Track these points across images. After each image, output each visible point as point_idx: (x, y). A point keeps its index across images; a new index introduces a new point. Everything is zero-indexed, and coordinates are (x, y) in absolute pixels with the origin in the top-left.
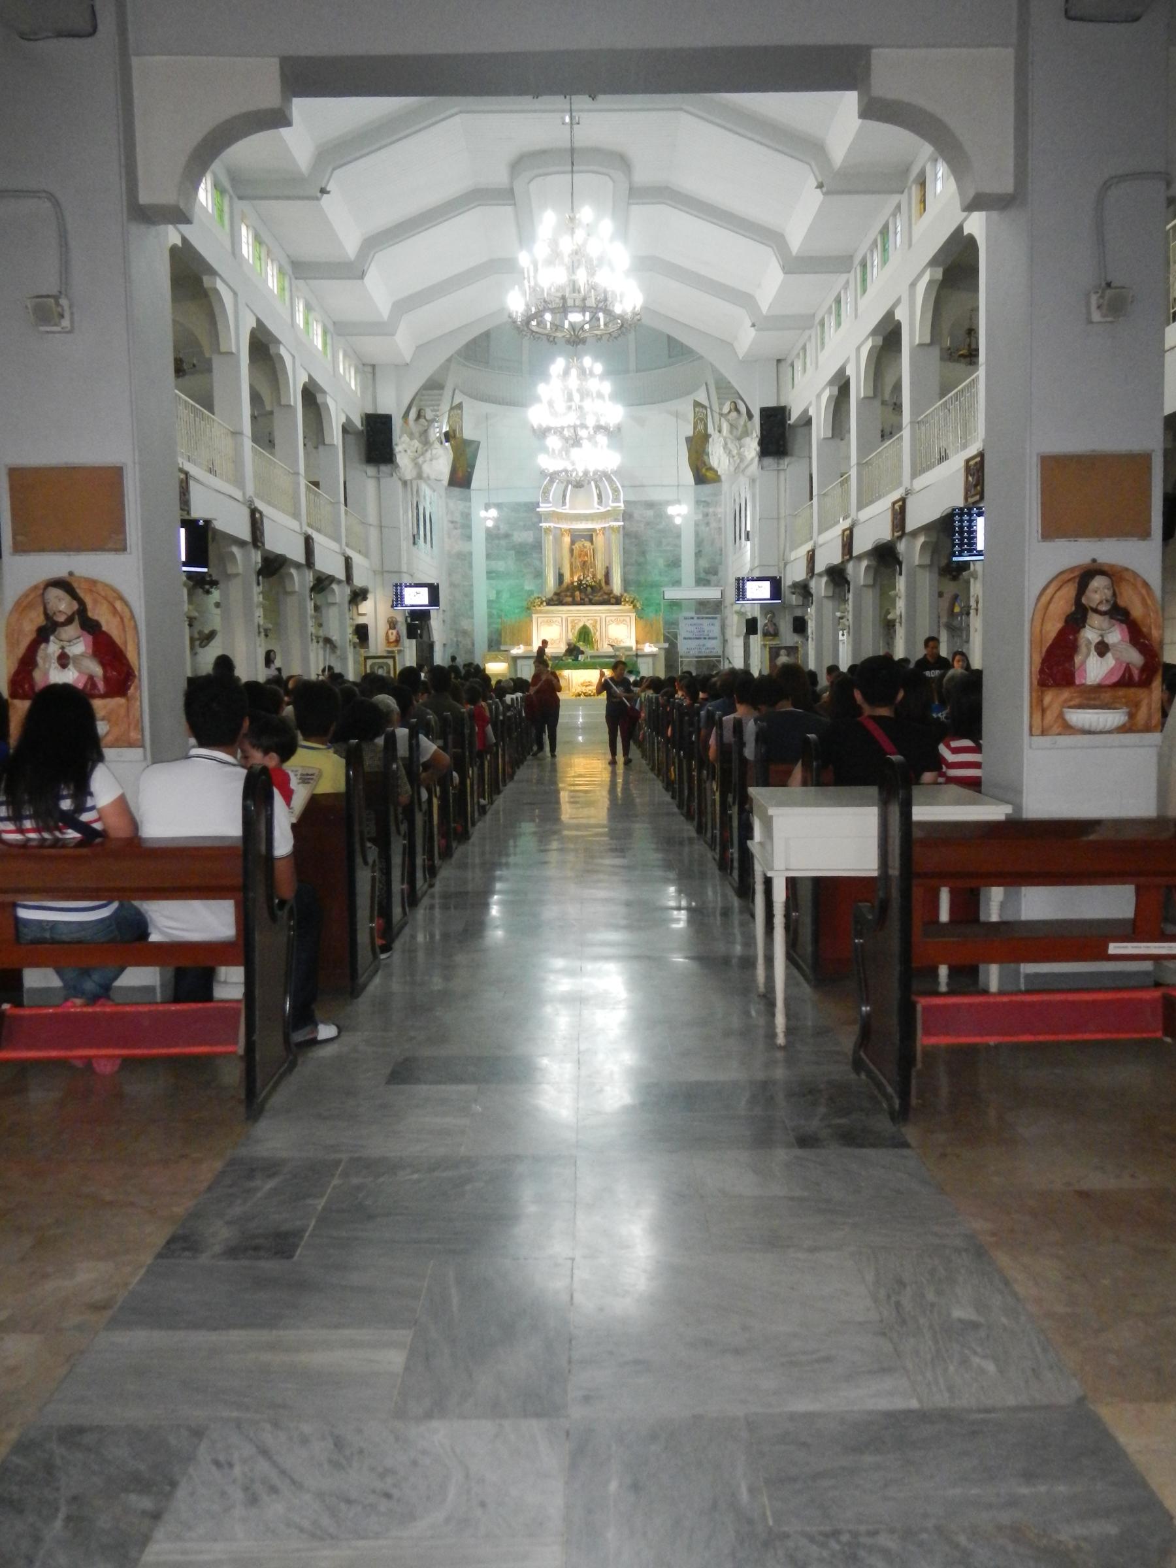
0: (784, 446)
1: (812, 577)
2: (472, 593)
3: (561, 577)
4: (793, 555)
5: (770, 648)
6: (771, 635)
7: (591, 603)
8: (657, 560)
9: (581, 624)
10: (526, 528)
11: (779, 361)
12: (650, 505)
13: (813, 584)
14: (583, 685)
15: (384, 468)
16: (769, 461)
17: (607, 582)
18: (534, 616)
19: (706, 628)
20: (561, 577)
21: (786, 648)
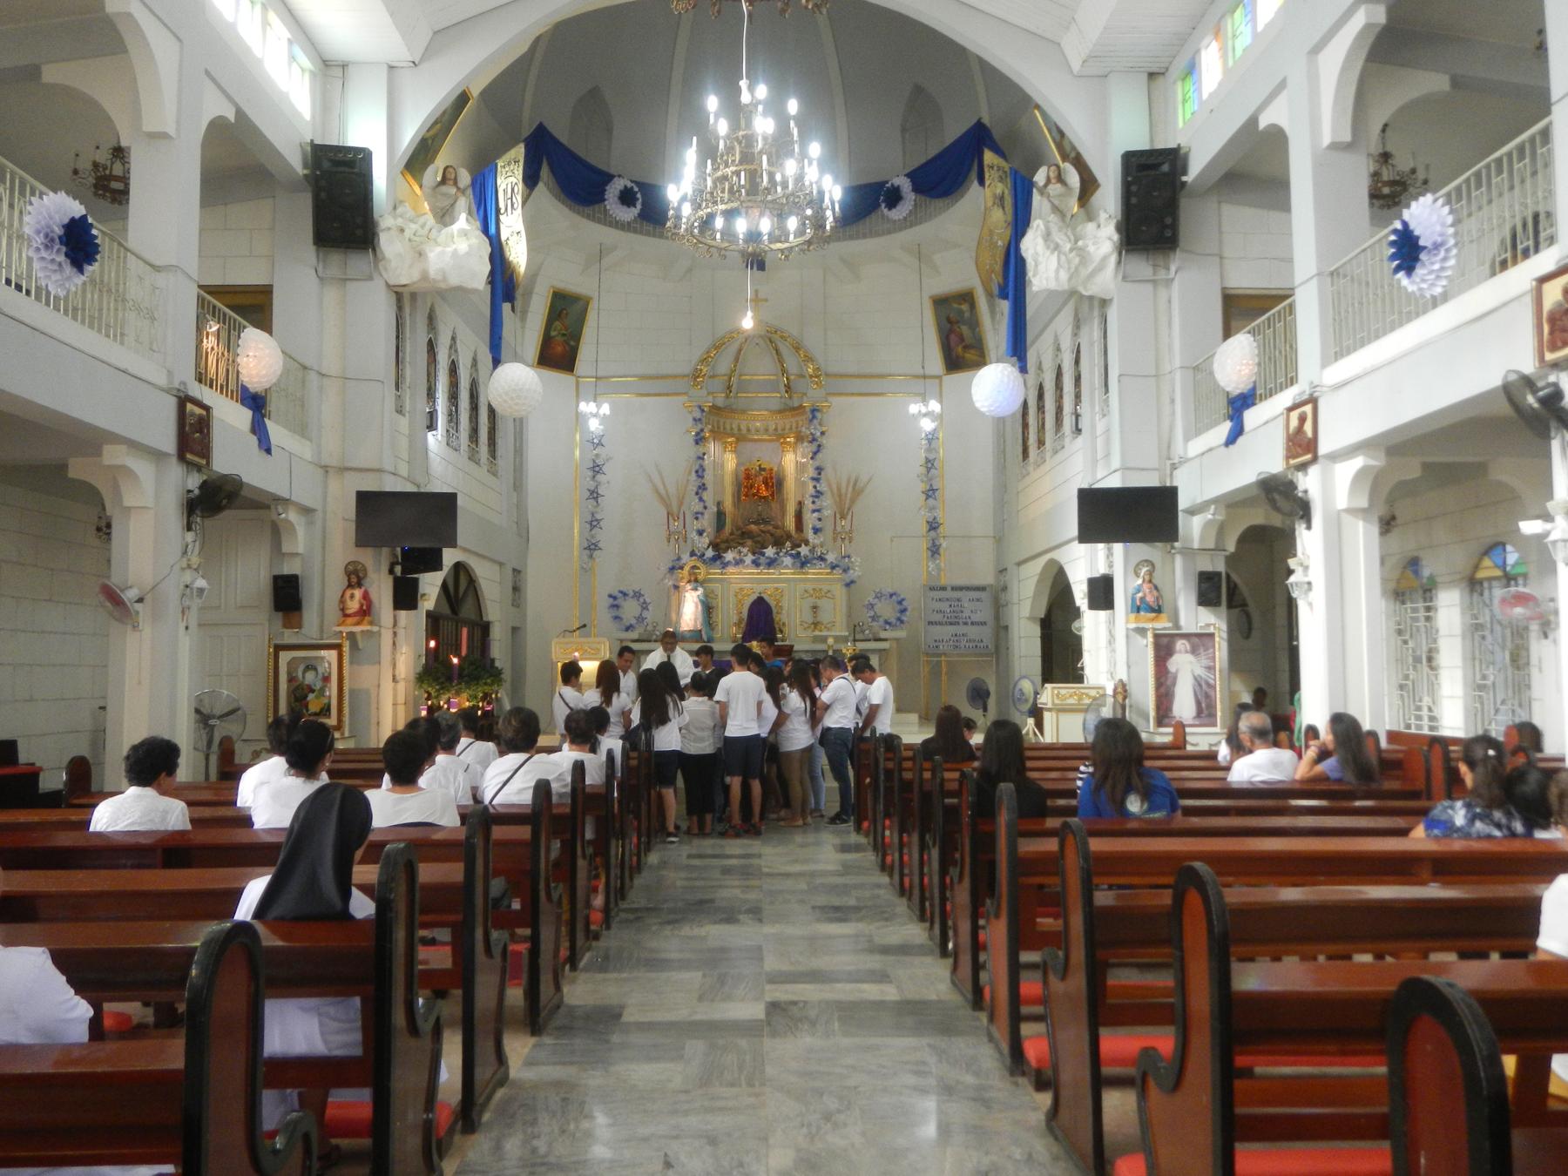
0: (1174, 227)
1: (1303, 467)
4: (1196, 446)
5: (1156, 636)
6: (1152, 610)
9: (754, 597)
11: (1152, 75)
13: (1309, 483)
15: (358, 262)
16: (1140, 266)
21: (1187, 636)
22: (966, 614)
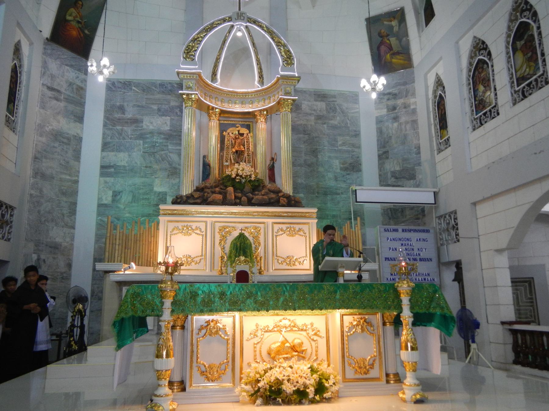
2: (75, 193)
3: (206, 167)
7: (250, 203)
8: (332, 162)
9: (236, 234)
10: (162, 113)
12: (321, 96)
14: (273, 355)
17: (272, 178)
18: (162, 219)
19: (416, 245)
20: (206, 166)
22: (416, 251)
